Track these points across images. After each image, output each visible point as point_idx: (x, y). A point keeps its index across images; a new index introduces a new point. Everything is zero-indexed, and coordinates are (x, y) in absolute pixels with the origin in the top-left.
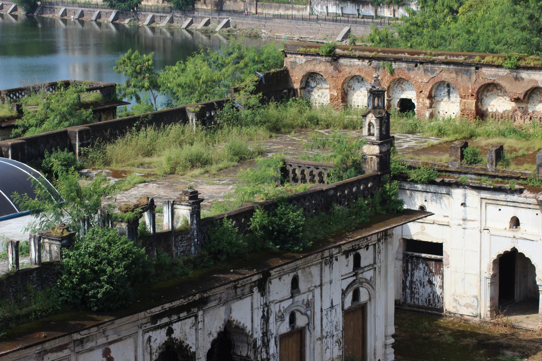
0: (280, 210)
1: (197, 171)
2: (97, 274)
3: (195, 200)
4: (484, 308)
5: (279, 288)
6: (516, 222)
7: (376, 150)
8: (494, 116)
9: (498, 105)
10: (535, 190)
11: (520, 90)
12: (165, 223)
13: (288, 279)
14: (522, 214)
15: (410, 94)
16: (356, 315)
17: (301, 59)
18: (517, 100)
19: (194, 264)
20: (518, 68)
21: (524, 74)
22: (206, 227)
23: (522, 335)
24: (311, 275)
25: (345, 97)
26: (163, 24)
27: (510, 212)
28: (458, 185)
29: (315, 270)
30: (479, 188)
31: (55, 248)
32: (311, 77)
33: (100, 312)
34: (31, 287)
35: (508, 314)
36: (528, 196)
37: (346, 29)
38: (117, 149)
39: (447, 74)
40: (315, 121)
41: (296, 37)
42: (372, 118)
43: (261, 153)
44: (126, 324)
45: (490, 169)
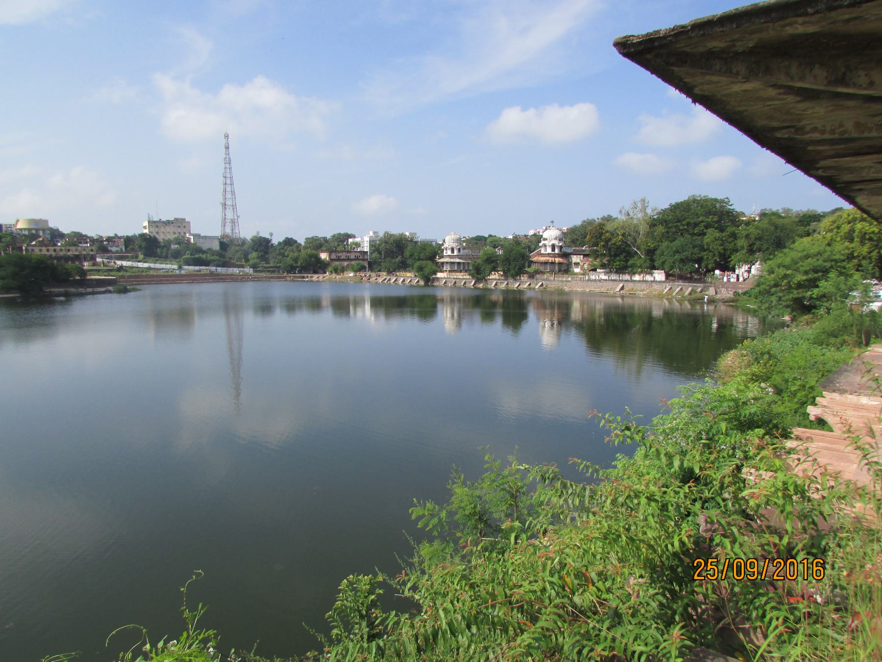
37: (621, 285)
41: (588, 290)
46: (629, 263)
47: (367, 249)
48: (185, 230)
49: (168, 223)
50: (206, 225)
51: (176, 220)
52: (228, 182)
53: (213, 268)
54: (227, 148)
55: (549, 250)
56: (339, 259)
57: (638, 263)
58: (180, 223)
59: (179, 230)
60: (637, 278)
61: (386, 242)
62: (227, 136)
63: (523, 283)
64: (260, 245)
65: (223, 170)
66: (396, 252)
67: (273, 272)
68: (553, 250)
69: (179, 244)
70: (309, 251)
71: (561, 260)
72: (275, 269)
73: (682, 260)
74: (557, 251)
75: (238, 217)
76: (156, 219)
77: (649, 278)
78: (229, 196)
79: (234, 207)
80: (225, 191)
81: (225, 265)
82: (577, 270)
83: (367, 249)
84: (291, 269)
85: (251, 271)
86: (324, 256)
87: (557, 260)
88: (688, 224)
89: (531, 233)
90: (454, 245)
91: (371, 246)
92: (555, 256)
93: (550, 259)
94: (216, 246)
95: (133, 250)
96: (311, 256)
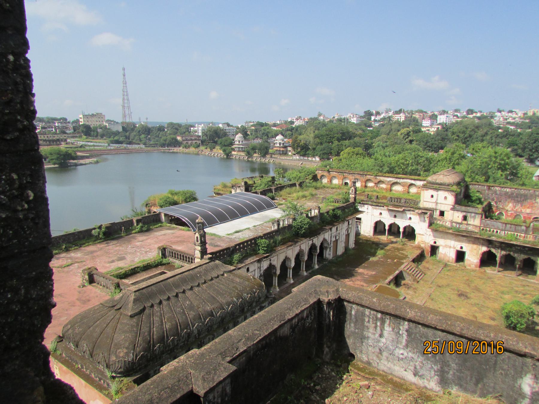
0: (336, 210)
1: (304, 199)
2: (301, 227)
3: (319, 208)
4: (371, 233)
5: (334, 229)
6: (381, 214)
7: (353, 196)
8: (369, 187)
9: (370, 184)
10: (387, 206)
11: (376, 181)
12: (313, 214)
13: (336, 227)
14: (382, 212)
15: (348, 181)
16: (348, 236)
17: (320, 172)
18: (375, 183)
19: (319, 224)
20: (377, 176)
21: (378, 178)
22: (321, 214)
23: (382, 242)
24: (340, 226)
25: (331, 181)
26: (259, 160)
27: (380, 211)
28: (366, 204)
29: (341, 225)
30: (372, 205)
31: (291, 221)
32: (322, 176)
33: (301, 237)
34: (286, 231)
35: (378, 235)
36: (385, 208)
38: (283, 192)
39: (357, 177)
40: (324, 187)
42: (353, 188)
43: (316, 195)
44: (305, 240)
45: (375, 201)
46: (307, 153)
47: (200, 134)
48: (102, 120)
49: (93, 115)
50: (114, 114)
51: (98, 114)
52: (125, 94)
53: (125, 145)
54: (124, 75)
55: (278, 145)
56: (187, 140)
57: (310, 153)
58: (99, 115)
59: (99, 119)
60: (310, 159)
61: (210, 131)
62: (124, 69)
63: (267, 159)
64: (146, 131)
65: (122, 88)
66: (216, 137)
67: (154, 146)
68: (280, 145)
69: (101, 128)
70: (172, 136)
71: (283, 149)
72: (155, 145)
73: (323, 154)
74: (281, 145)
75: (131, 113)
76: (86, 114)
77: (314, 159)
78: (126, 101)
79: (129, 107)
80: (124, 99)
81: (130, 143)
82: (290, 154)
83: (200, 134)
84: (163, 145)
85: (142, 146)
86: (179, 138)
87: (281, 149)
88: (330, 137)
89: (289, 120)
90: (240, 139)
91: (203, 133)
92: (280, 147)
93: (279, 149)
94: (120, 129)
95: (79, 133)
96: (173, 139)
